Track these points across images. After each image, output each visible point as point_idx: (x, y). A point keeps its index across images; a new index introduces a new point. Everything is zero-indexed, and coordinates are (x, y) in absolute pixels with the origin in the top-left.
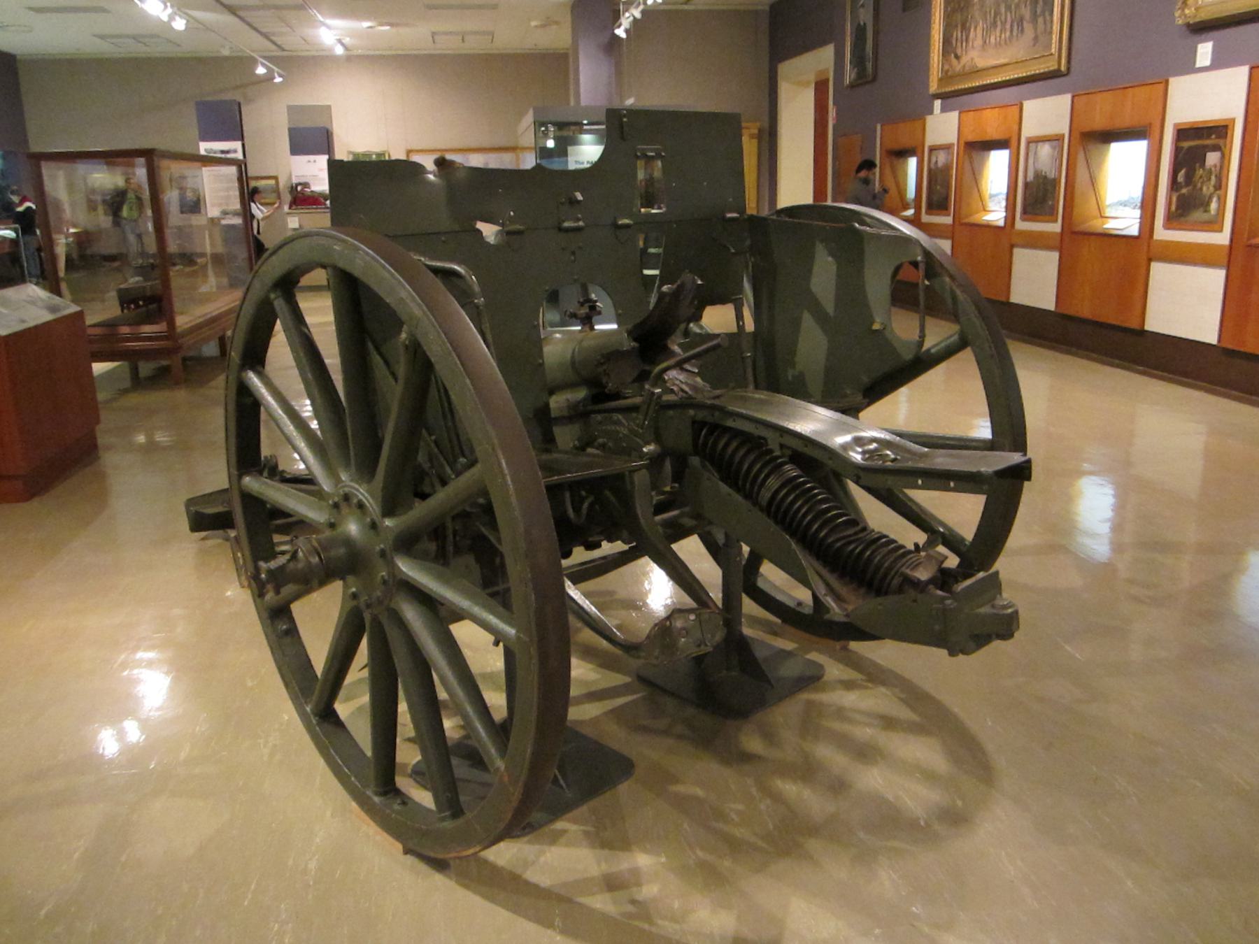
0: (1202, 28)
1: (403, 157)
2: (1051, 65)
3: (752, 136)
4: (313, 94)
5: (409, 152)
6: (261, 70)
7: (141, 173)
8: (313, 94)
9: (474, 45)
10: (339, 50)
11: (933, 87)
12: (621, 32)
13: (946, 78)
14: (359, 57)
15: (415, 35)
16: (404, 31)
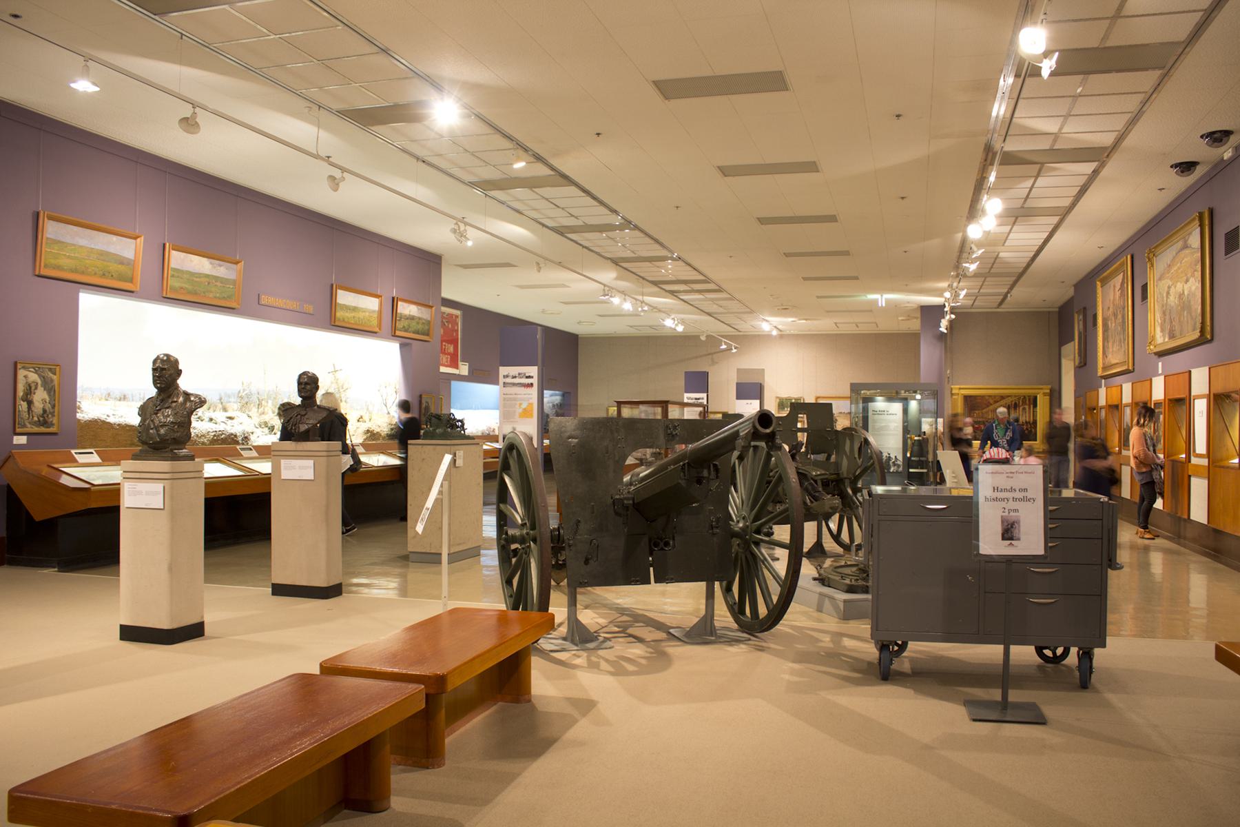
0: (1161, 354)
1: (813, 401)
2: (1124, 368)
3: (1045, 394)
4: (751, 361)
5: (817, 398)
6: (724, 347)
7: (659, 410)
8: (751, 361)
9: (865, 329)
10: (775, 333)
11: (1100, 373)
12: (943, 329)
13: (1105, 368)
14: (789, 335)
15: (824, 324)
16: (816, 322)
